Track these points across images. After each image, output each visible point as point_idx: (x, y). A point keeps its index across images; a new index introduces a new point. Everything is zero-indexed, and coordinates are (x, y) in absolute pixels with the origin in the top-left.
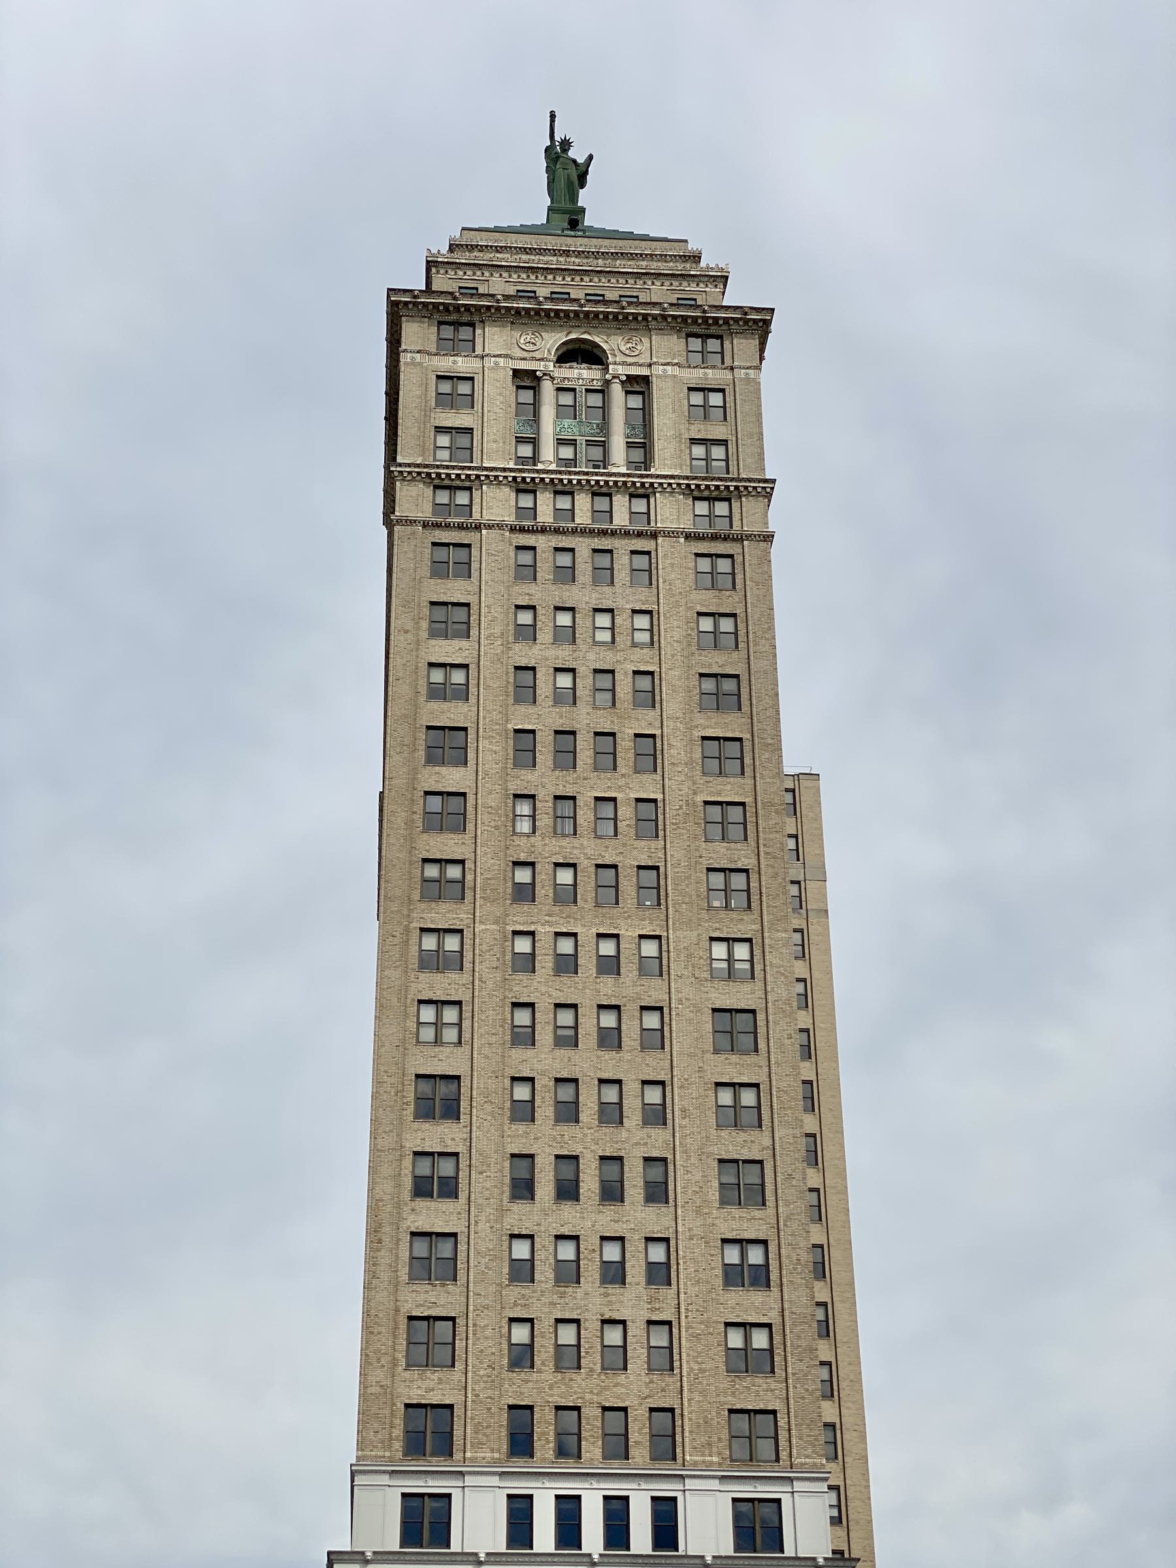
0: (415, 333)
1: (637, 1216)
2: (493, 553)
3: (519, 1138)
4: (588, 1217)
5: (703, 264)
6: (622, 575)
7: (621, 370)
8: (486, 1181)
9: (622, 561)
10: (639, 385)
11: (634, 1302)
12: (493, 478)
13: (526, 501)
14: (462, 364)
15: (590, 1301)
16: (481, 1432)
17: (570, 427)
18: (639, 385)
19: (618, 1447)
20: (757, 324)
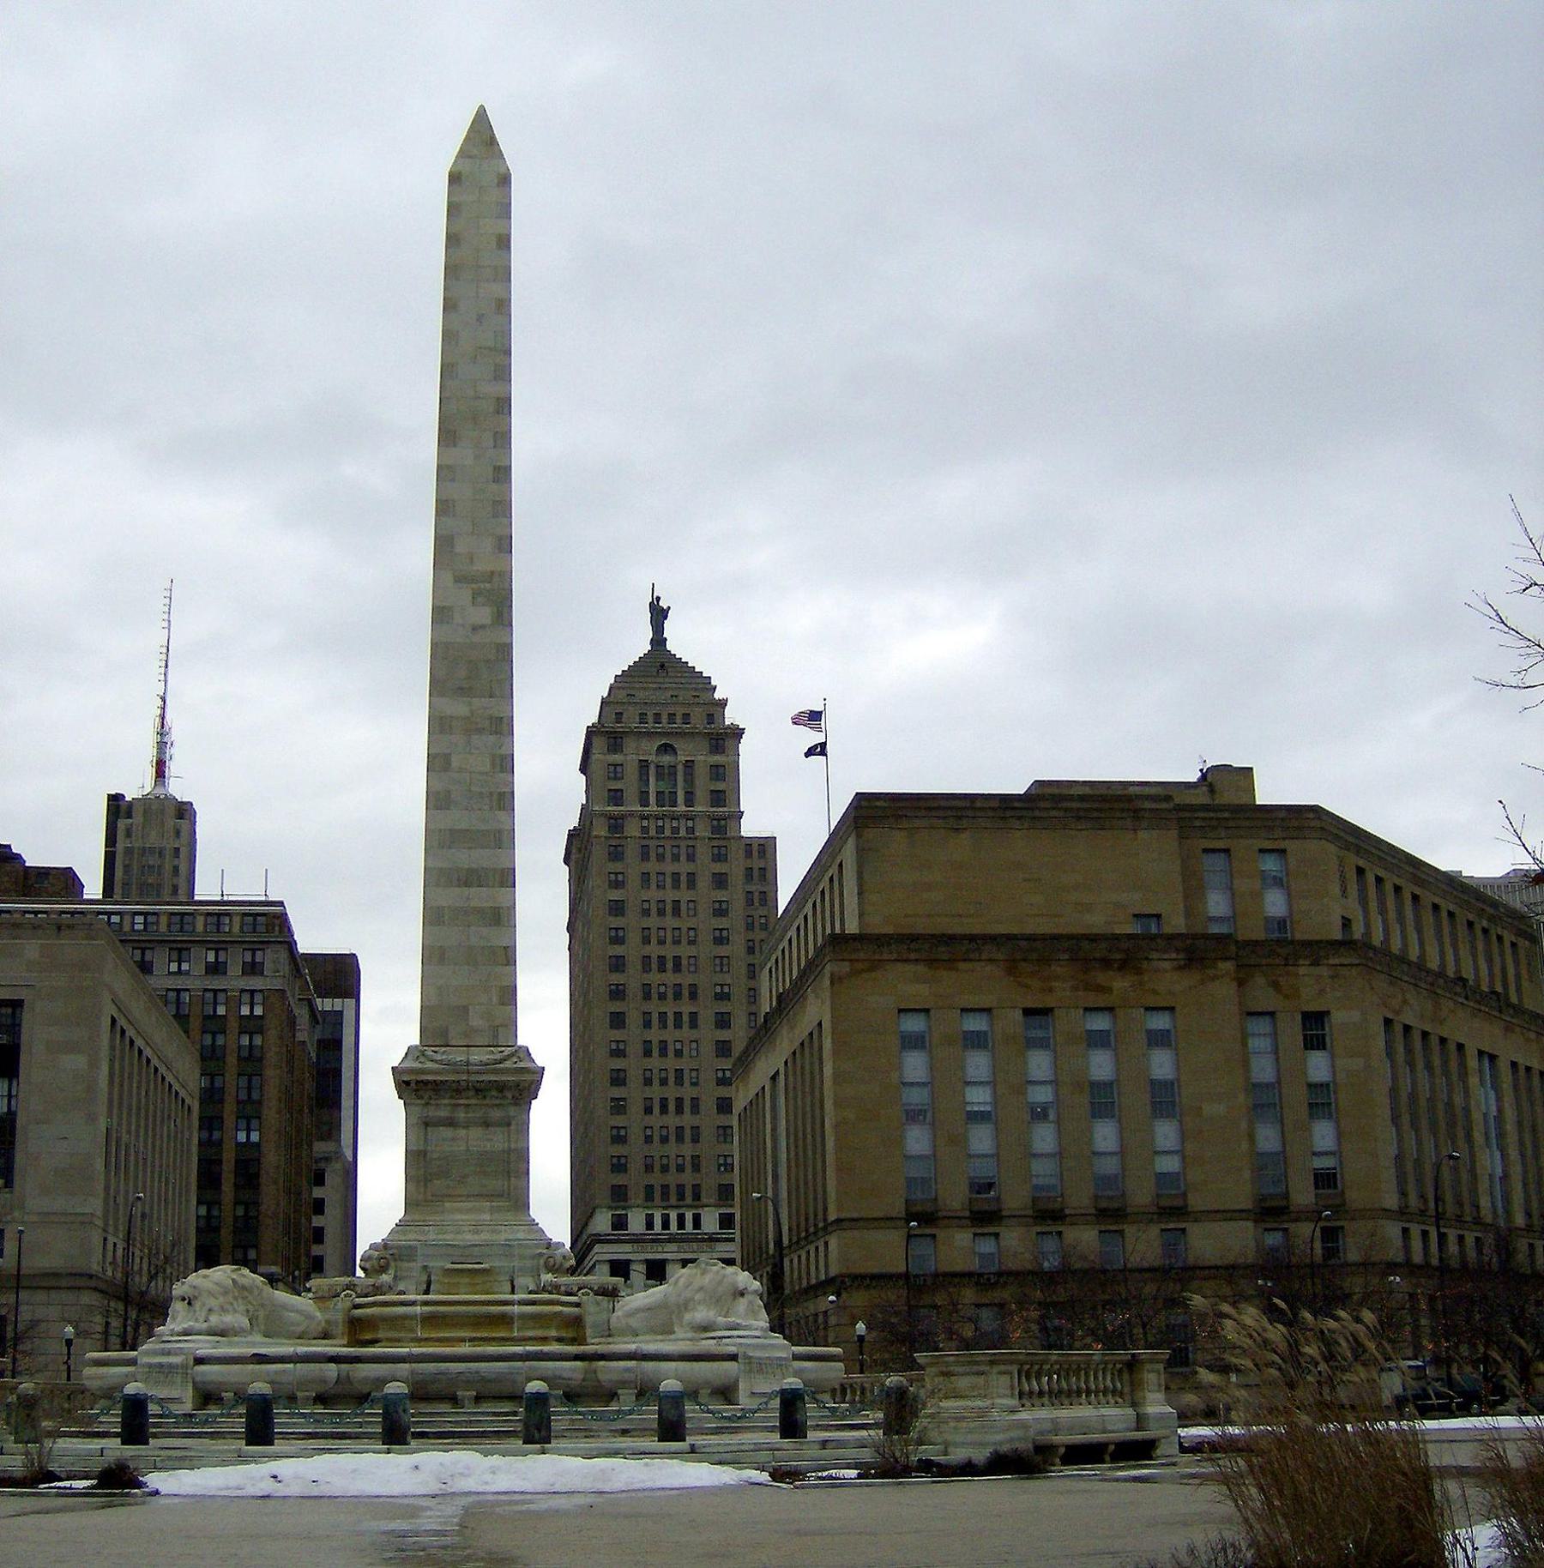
0: (596, 741)
1: (687, 1119)
2: (632, 850)
3: (648, 1092)
4: (672, 1120)
5: (717, 696)
6: (683, 858)
7: (683, 759)
8: (636, 1108)
9: (683, 850)
10: (689, 765)
11: (688, 1150)
12: (631, 814)
13: (645, 823)
14: (617, 758)
15: (672, 1149)
16: (635, 1195)
17: (663, 786)
18: (689, 765)
19: (681, 1197)
20: (737, 733)
